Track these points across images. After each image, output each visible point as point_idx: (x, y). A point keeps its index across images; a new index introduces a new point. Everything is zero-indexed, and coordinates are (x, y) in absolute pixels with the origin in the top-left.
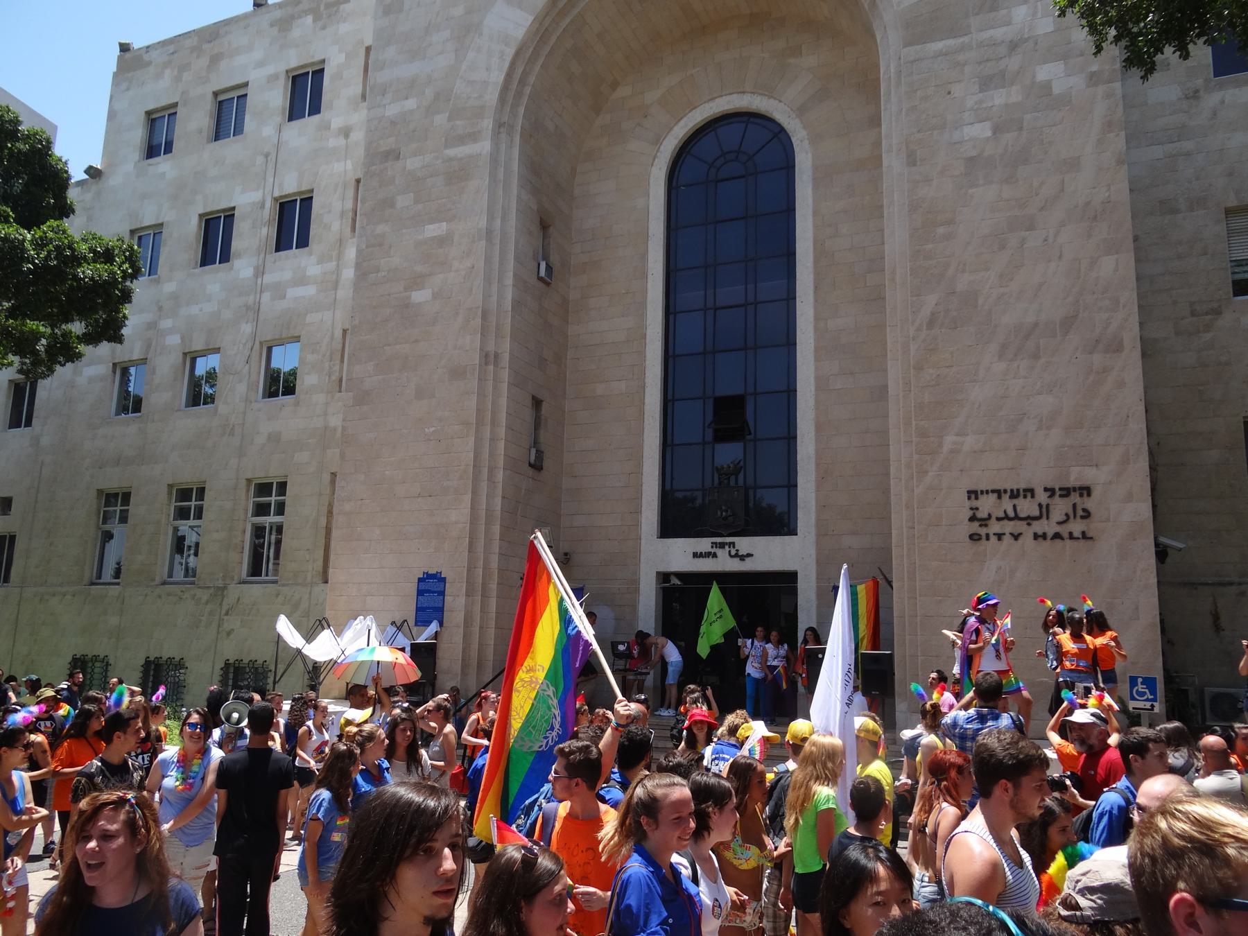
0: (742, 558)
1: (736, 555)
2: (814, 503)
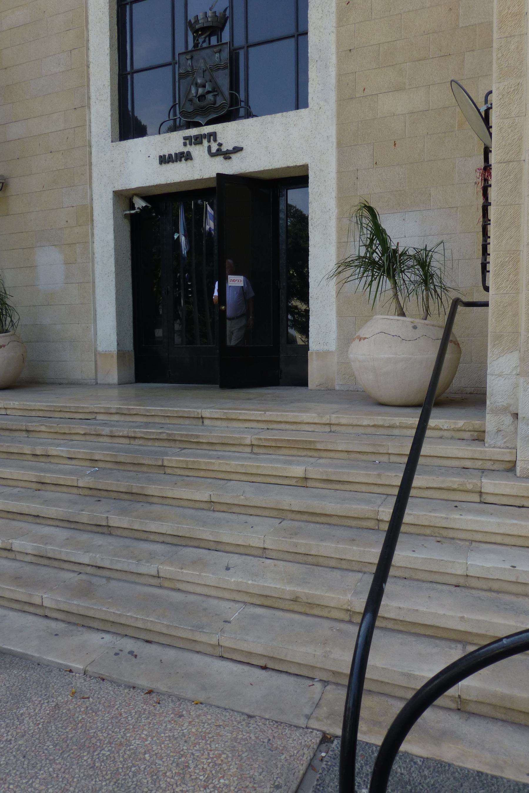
0: (227, 155)
1: (219, 153)
2: (333, 49)
